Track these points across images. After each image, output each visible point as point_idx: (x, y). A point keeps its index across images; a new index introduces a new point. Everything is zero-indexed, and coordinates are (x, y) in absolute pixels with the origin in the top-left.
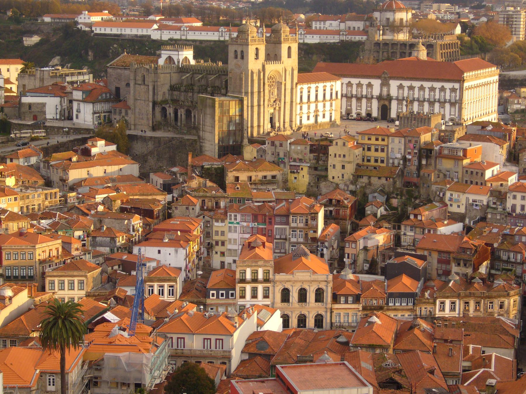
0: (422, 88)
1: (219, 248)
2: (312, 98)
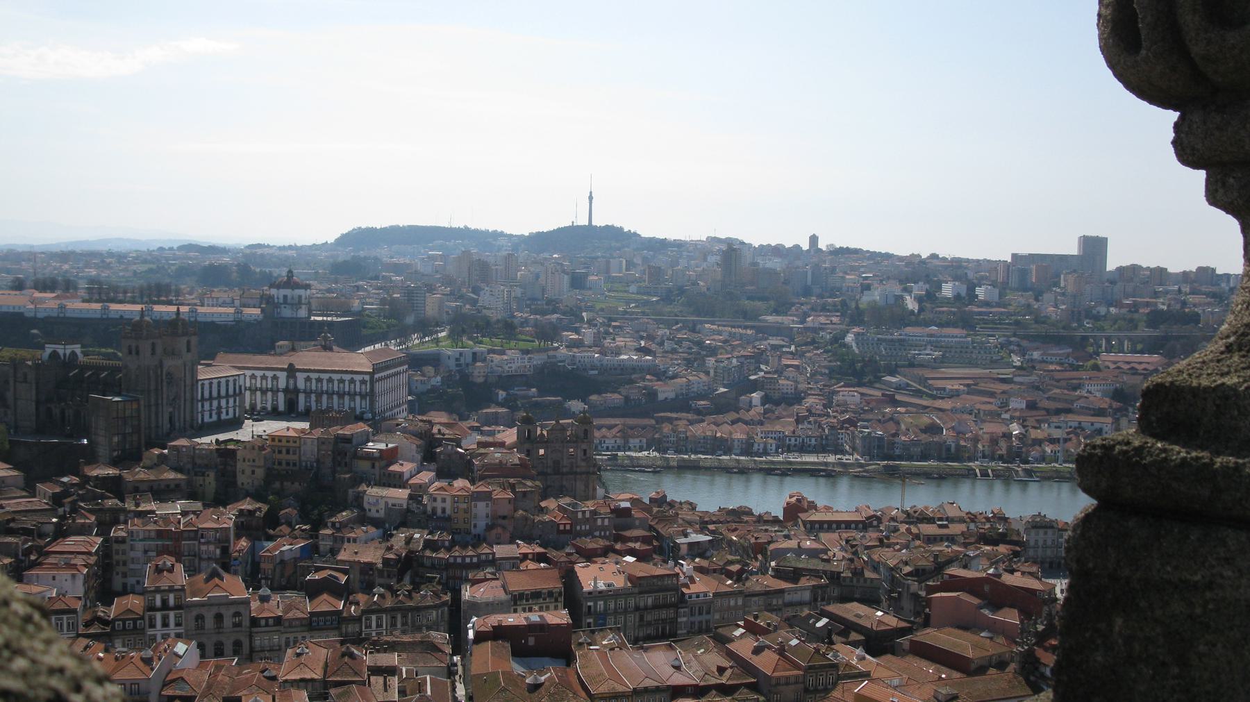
0: (330, 380)
1: (120, 569)
2: (215, 394)
